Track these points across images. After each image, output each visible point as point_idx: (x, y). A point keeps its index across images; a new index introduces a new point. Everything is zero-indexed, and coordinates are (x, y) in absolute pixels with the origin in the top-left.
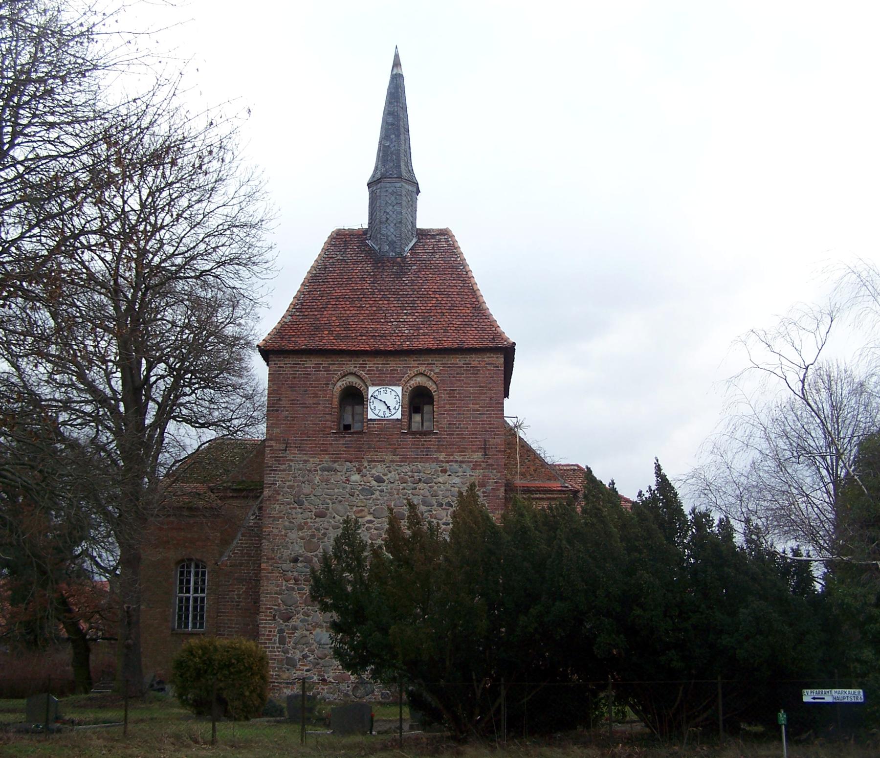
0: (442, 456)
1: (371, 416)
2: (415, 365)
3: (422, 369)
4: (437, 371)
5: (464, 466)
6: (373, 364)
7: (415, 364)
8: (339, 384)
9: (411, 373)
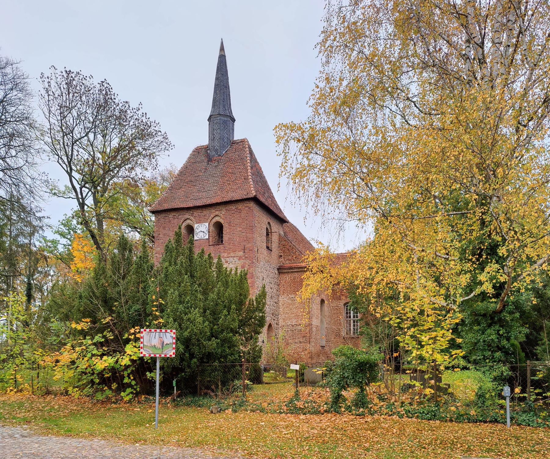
0: (226, 255)
1: (196, 238)
2: (213, 212)
3: (217, 213)
4: (223, 213)
5: (235, 258)
6: (196, 213)
7: (214, 211)
8: (184, 224)
9: (212, 216)
